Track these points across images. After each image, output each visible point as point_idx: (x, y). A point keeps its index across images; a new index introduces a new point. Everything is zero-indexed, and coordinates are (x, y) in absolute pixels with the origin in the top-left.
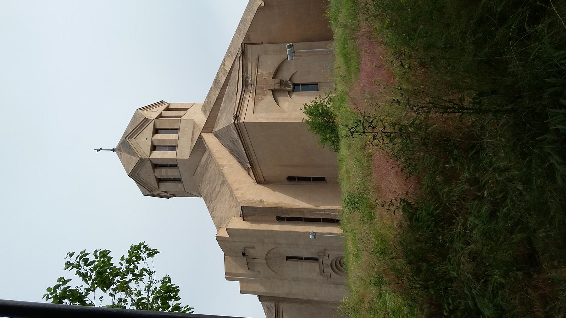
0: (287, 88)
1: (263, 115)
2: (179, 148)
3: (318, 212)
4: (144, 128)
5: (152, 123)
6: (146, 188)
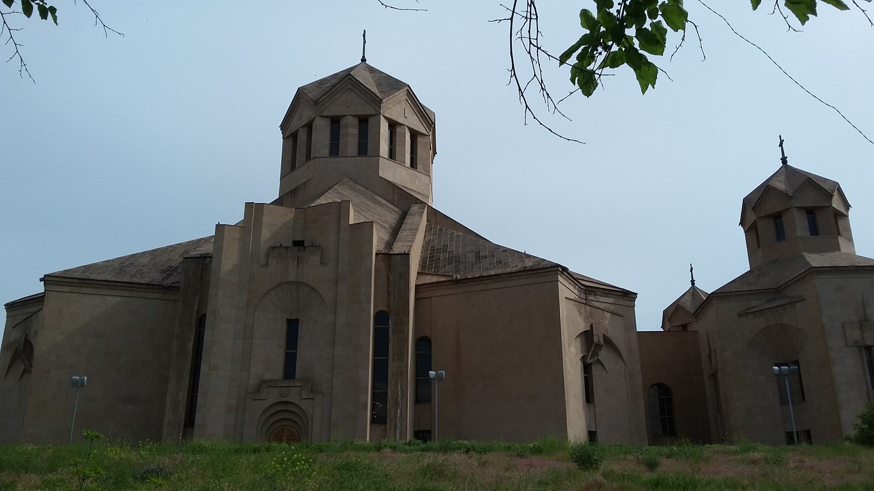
0: (590, 355)
1: (565, 314)
2: (391, 163)
3: (401, 387)
4: (419, 117)
5: (424, 132)
6: (325, 97)
